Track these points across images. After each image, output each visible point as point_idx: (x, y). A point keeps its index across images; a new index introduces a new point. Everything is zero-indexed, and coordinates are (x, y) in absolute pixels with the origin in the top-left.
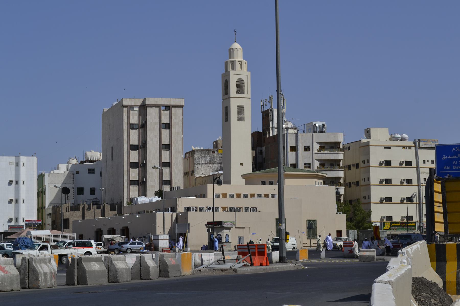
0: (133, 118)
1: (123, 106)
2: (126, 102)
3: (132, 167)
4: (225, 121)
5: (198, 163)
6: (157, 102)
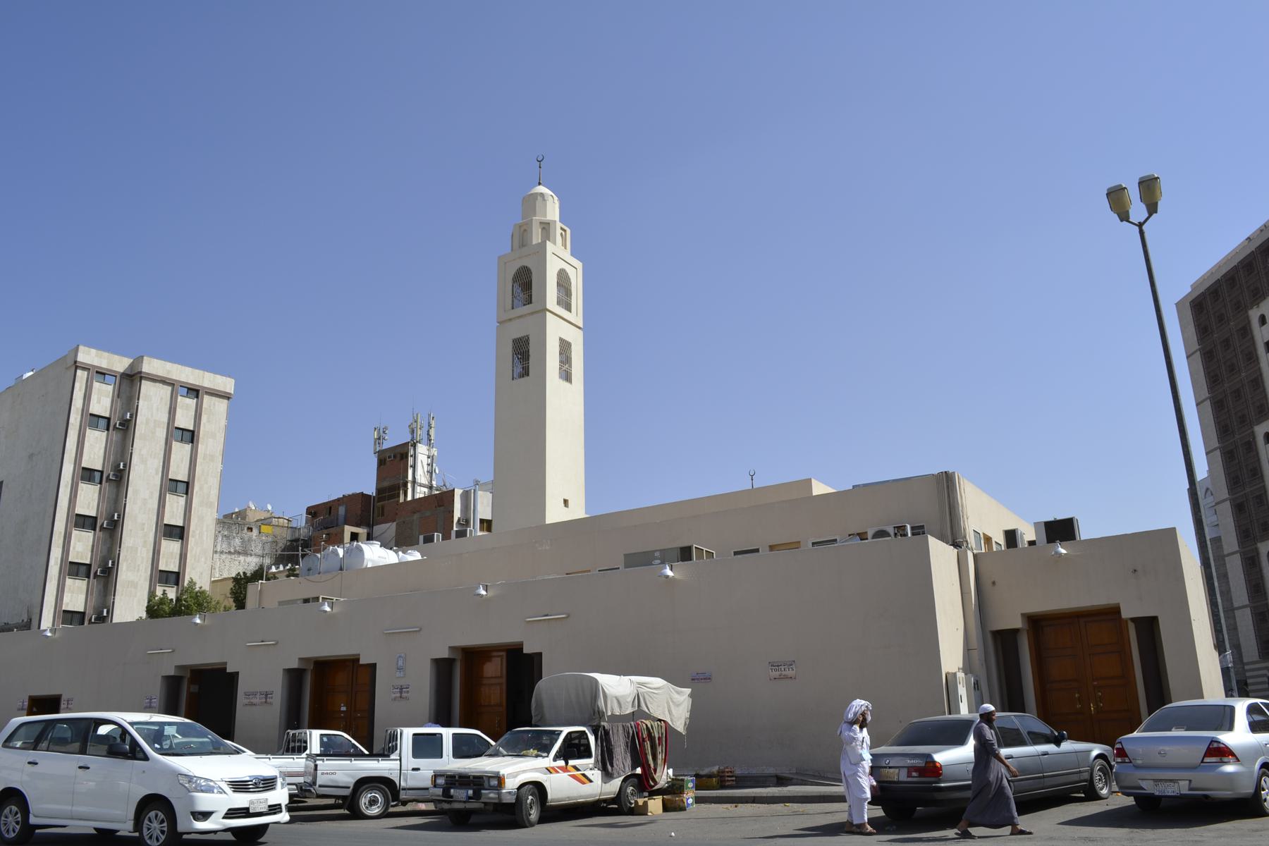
0: (99, 402)
1: (77, 366)
2: (87, 356)
3: (77, 525)
6: (169, 372)
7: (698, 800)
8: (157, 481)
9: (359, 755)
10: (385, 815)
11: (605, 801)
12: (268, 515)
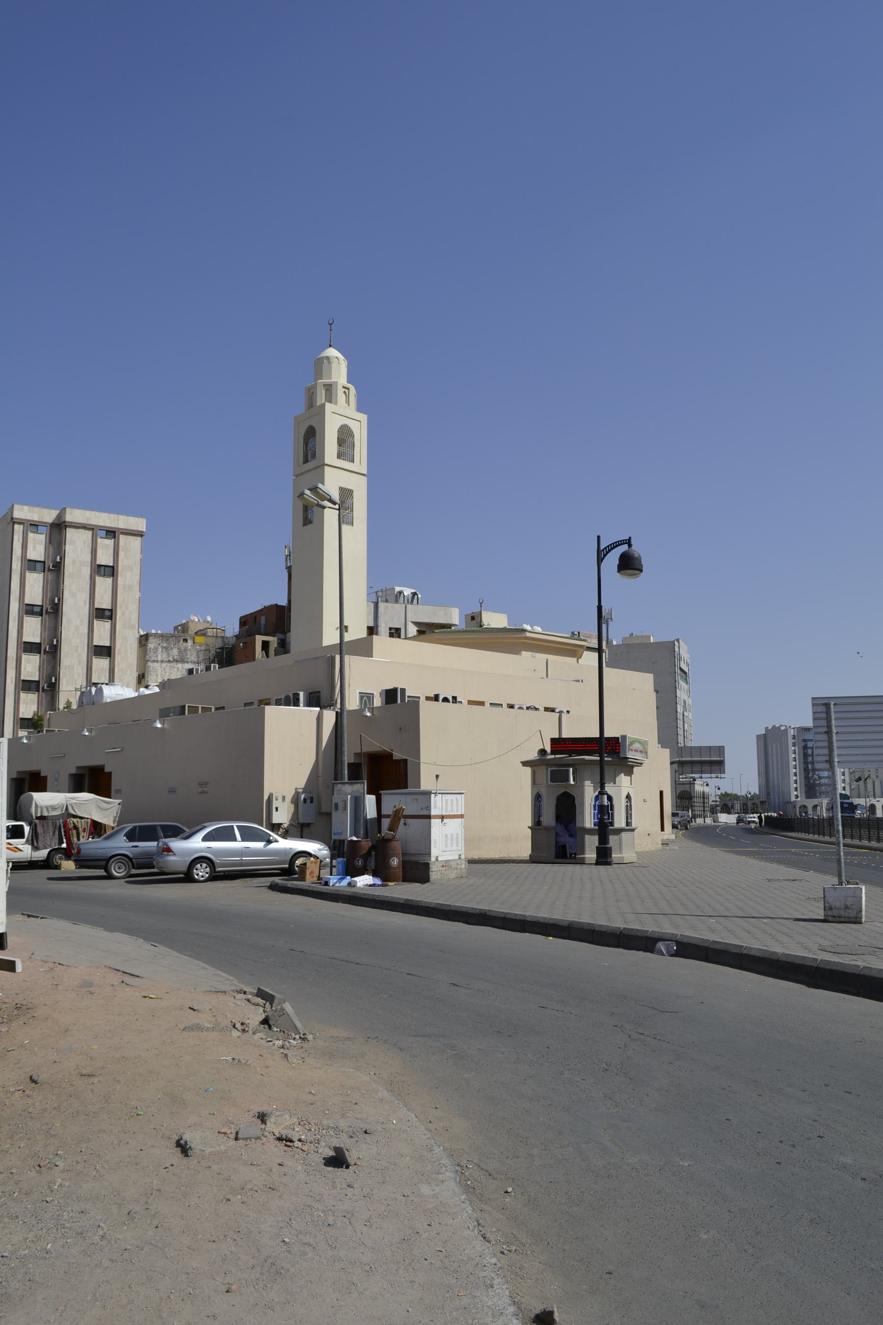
0: (34, 549)
1: (14, 522)
2: (21, 512)
3: (25, 651)
4: (305, 524)
5: (153, 658)
6: (88, 519)
8: (86, 611)
12: (208, 625)
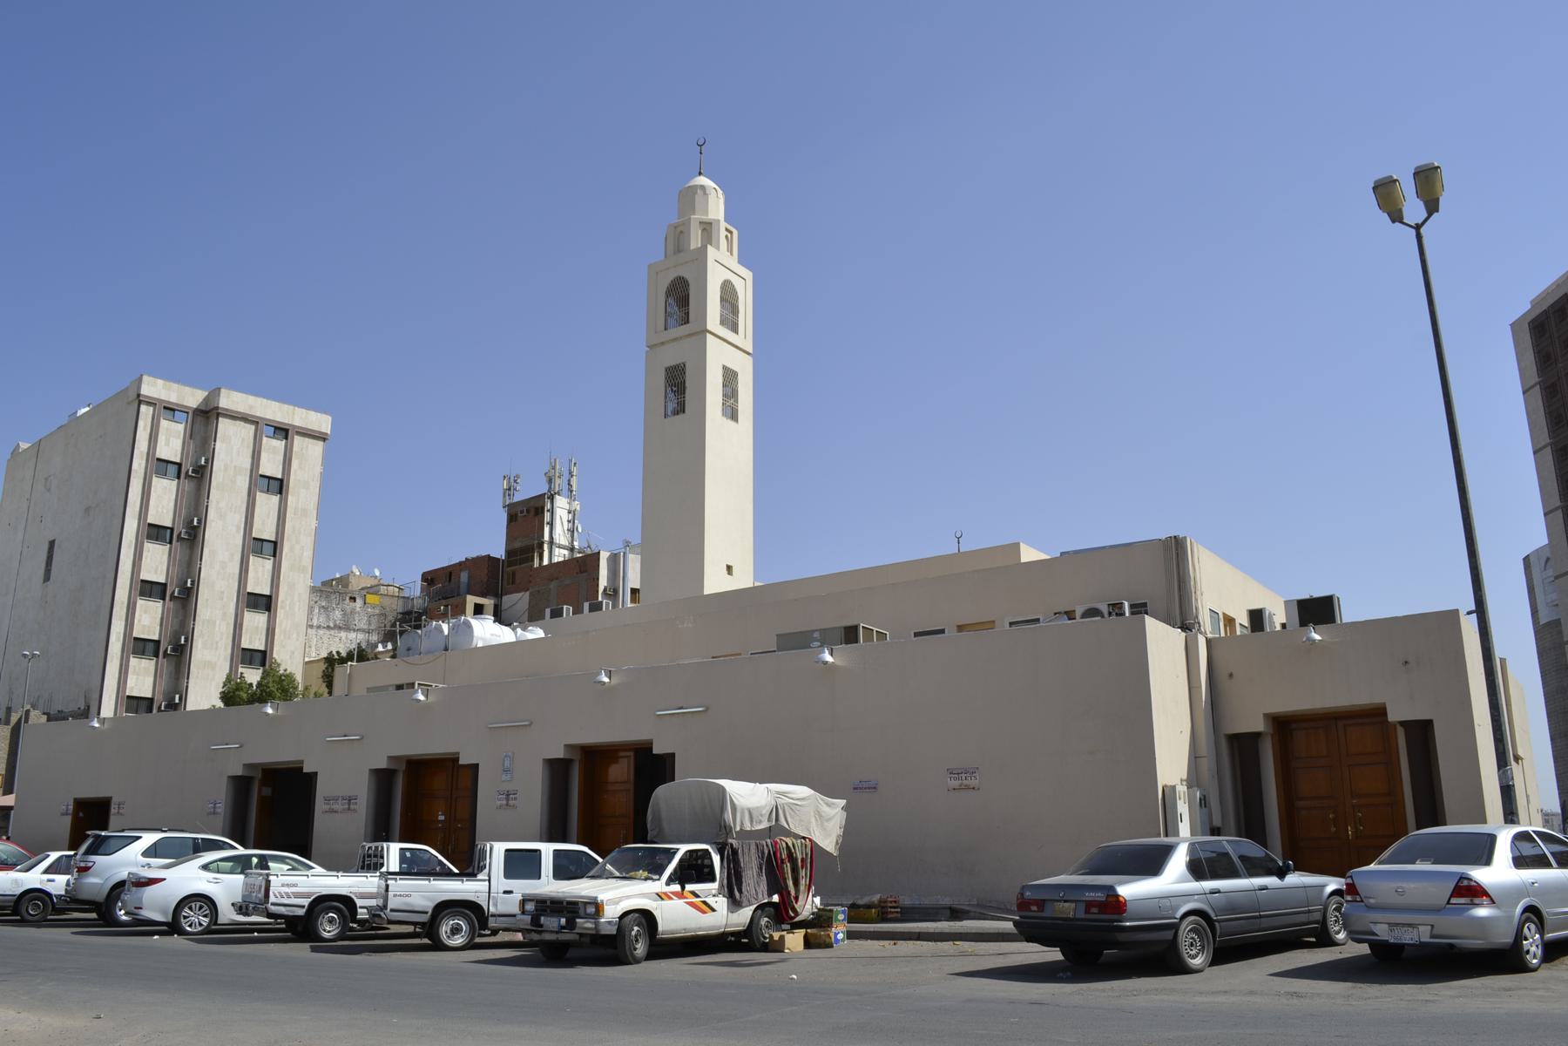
0: (167, 444)
1: (140, 400)
2: (153, 387)
3: (142, 594)
7: (851, 935)
8: (238, 540)
9: (448, 874)
10: (470, 946)
11: (732, 934)
12: (375, 582)
